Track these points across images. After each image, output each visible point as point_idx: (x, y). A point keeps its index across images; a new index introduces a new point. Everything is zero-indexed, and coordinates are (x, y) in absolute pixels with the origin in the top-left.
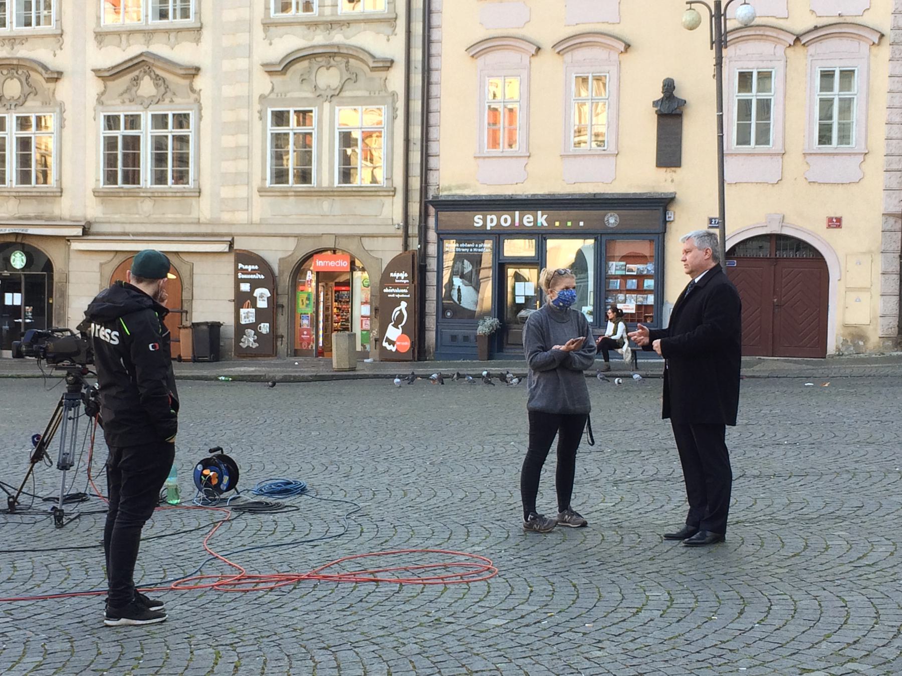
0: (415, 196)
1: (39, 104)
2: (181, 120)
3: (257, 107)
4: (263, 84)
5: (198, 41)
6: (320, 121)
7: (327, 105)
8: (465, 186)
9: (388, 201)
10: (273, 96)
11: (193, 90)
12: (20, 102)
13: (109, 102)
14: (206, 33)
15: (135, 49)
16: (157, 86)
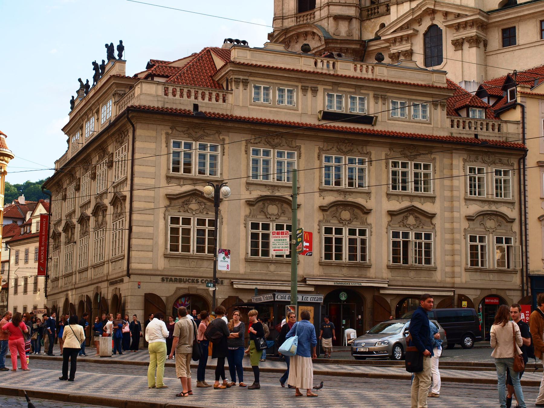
0: (525, 274)
1: (359, 223)
2: (428, 236)
3: (463, 234)
4: (465, 224)
5: (434, 203)
6: (489, 241)
7: (491, 235)
8: (539, 271)
9: (514, 275)
10: (469, 229)
11: (432, 224)
12: (350, 221)
13: (393, 226)
14: (437, 200)
15: (406, 204)
16: (416, 220)
